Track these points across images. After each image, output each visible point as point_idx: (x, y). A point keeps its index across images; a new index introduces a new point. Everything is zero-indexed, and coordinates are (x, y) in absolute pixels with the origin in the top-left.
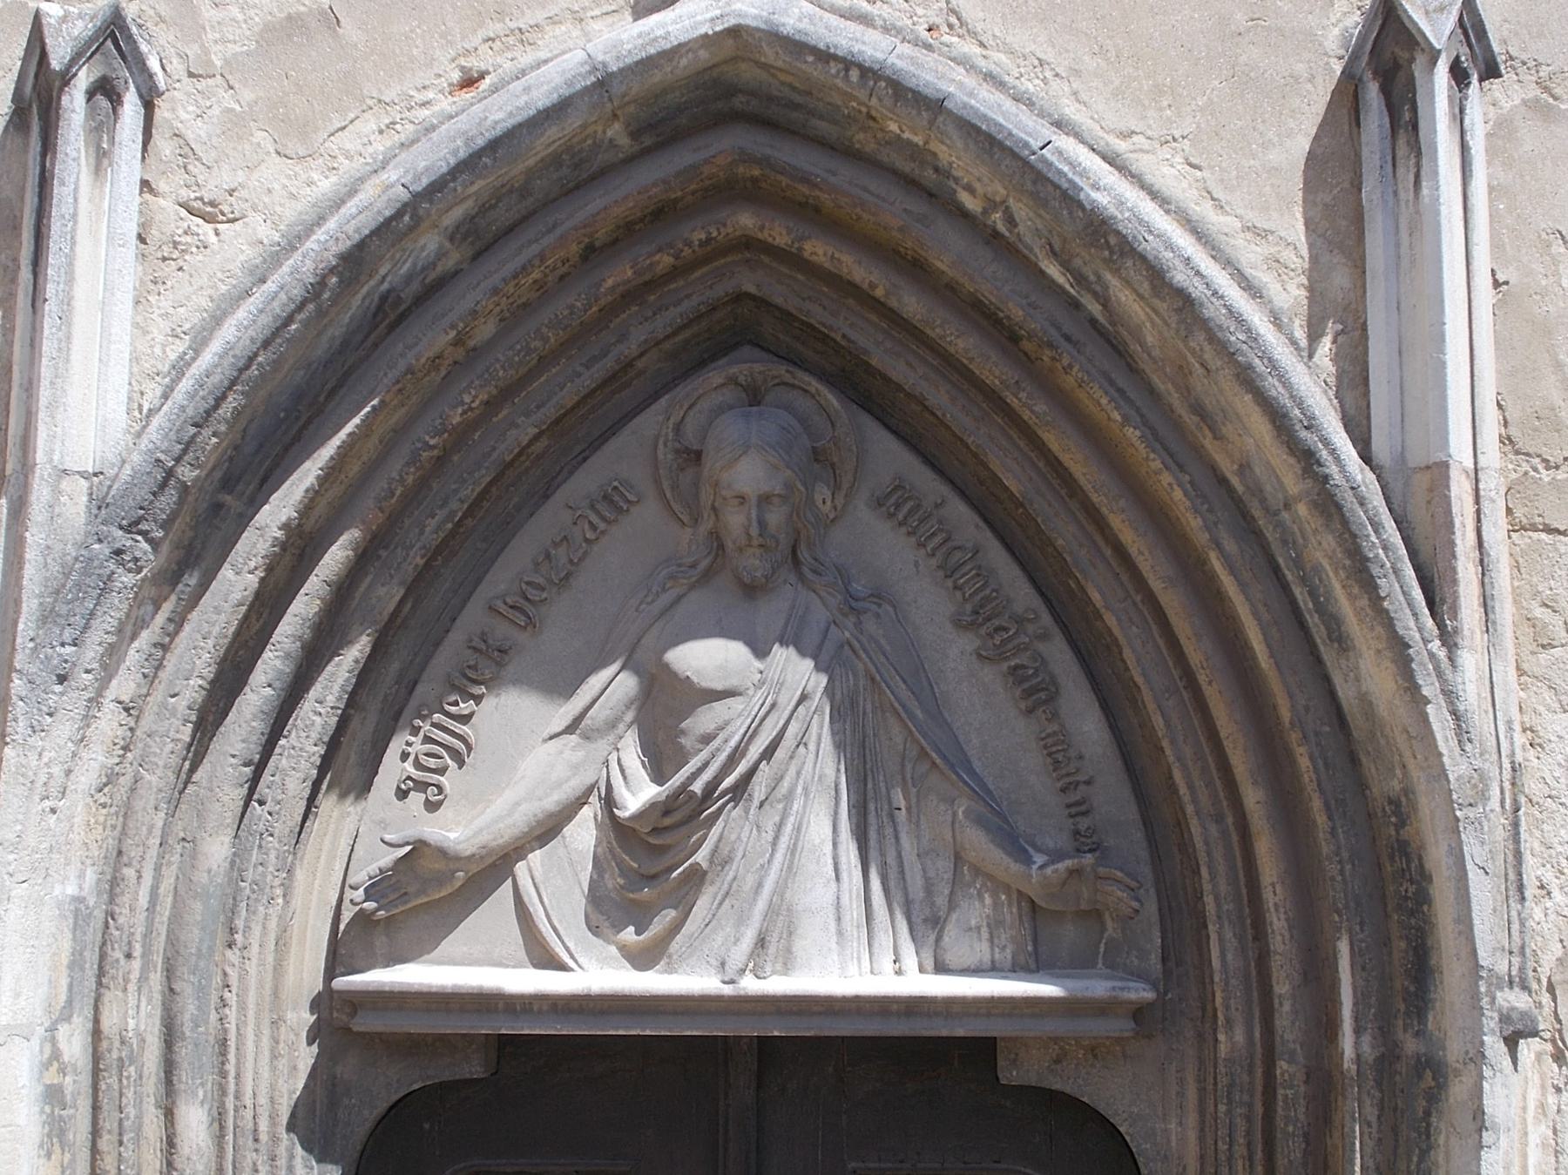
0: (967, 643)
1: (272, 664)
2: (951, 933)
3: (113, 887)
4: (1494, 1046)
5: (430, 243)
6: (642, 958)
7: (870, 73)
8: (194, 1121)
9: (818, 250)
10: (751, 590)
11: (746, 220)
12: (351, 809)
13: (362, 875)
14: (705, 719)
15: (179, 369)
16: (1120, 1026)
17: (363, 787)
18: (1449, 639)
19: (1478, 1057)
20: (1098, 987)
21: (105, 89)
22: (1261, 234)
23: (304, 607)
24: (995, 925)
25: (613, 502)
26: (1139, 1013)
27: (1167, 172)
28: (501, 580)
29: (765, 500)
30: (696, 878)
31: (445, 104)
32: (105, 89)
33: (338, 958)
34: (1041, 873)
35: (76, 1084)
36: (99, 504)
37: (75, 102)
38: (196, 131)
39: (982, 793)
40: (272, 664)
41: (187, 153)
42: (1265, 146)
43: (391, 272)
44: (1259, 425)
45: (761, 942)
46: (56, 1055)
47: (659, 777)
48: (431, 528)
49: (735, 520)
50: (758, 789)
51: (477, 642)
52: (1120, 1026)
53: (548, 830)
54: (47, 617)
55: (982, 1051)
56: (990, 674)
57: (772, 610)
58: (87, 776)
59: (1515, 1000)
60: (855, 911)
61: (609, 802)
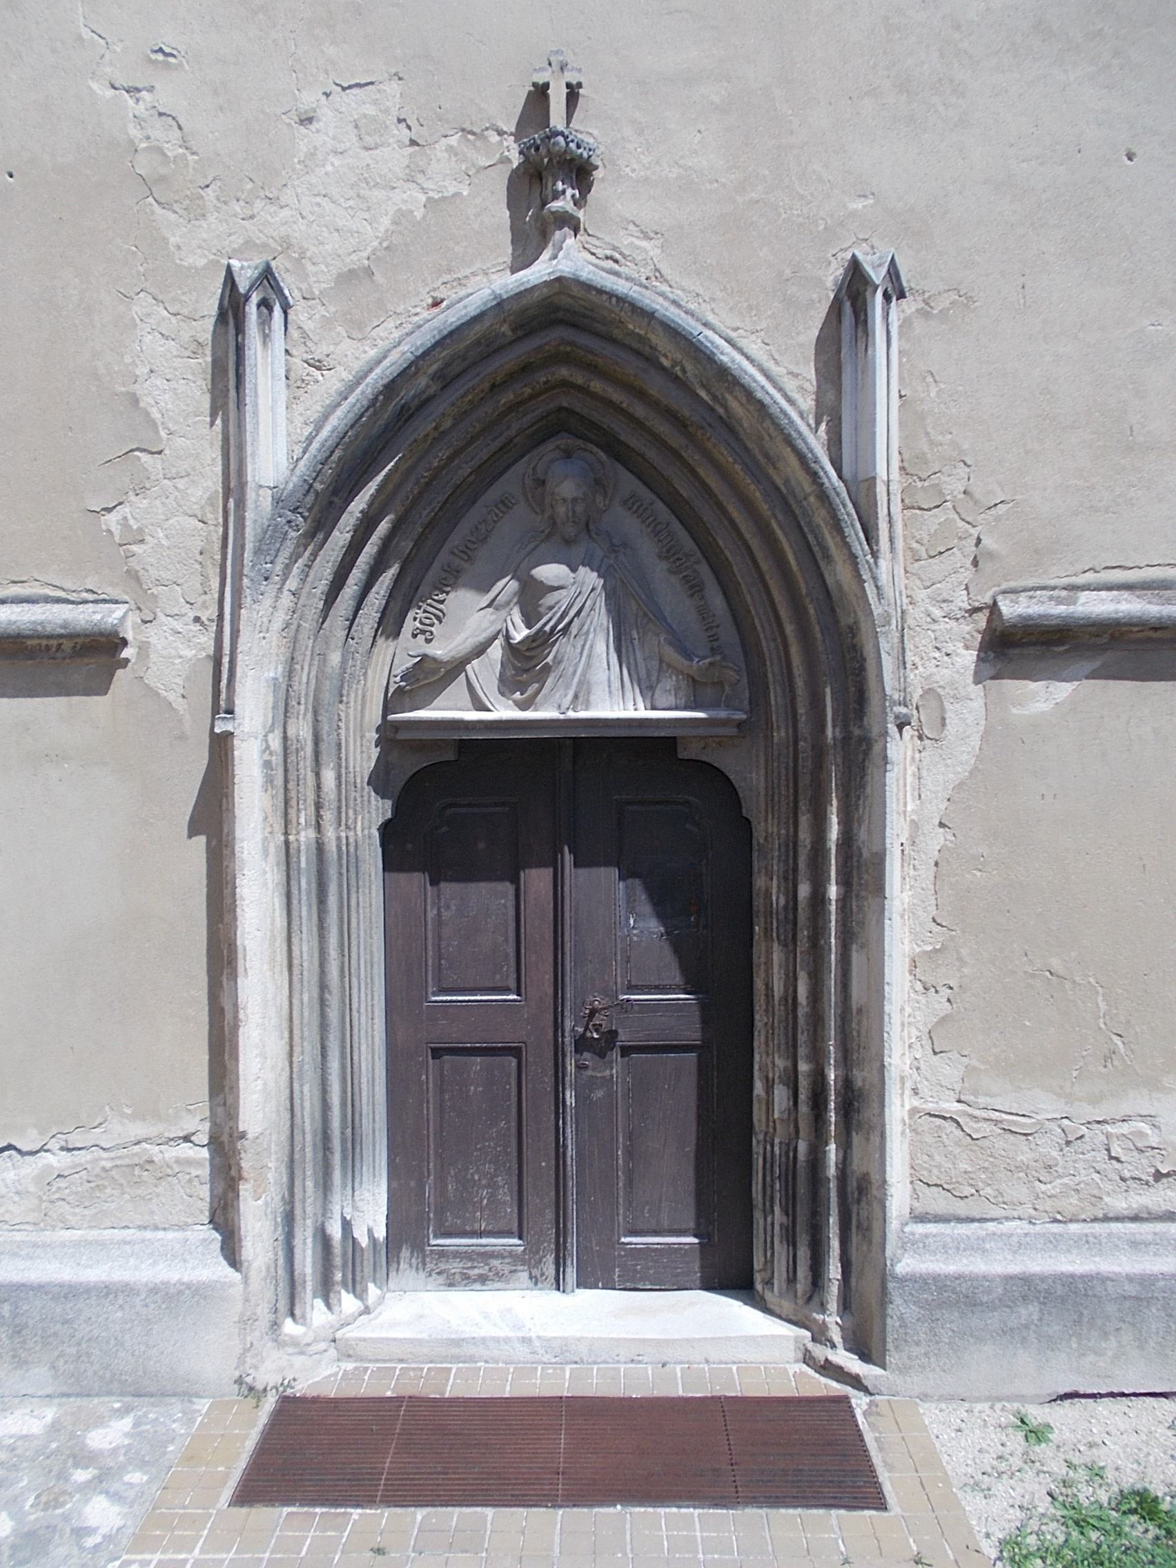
0: (664, 565)
1: (357, 575)
2: (658, 692)
3: (290, 674)
4: (892, 728)
5: (423, 381)
6: (523, 706)
7: (621, 300)
8: (329, 776)
9: (597, 386)
10: (568, 542)
11: (564, 372)
12: (392, 644)
13: (398, 670)
14: (550, 599)
15: (310, 440)
16: (731, 731)
17: (396, 634)
18: (875, 555)
19: (885, 733)
20: (722, 714)
21: (265, 304)
22: (796, 376)
23: (370, 549)
24: (677, 689)
25: (505, 504)
26: (740, 725)
28: (455, 540)
29: (575, 500)
30: (547, 669)
31: (426, 314)
33: (387, 709)
34: (696, 666)
35: (277, 760)
36: (277, 501)
37: (252, 309)
38: (309, 326)
39: (670, 630)
40: (357, 575)
41: (305, 336)
42: (798, 334)
43: (406, 394)
44: (793, 461)
45: (576, 697)
46: (268, 747)
47: (529, 627)
48: (425, 515)
49: (561, 510)
50: (574, 629)
51: (446, 568)
52: (731, 731)
53: (480, 650)
54: (257, 551)
55: (670, 744)
56: (674, 580)
57: (579, 551)
58: (277, 624)
59: (903, 710)
60: (616, 683)
61: (508, 637)
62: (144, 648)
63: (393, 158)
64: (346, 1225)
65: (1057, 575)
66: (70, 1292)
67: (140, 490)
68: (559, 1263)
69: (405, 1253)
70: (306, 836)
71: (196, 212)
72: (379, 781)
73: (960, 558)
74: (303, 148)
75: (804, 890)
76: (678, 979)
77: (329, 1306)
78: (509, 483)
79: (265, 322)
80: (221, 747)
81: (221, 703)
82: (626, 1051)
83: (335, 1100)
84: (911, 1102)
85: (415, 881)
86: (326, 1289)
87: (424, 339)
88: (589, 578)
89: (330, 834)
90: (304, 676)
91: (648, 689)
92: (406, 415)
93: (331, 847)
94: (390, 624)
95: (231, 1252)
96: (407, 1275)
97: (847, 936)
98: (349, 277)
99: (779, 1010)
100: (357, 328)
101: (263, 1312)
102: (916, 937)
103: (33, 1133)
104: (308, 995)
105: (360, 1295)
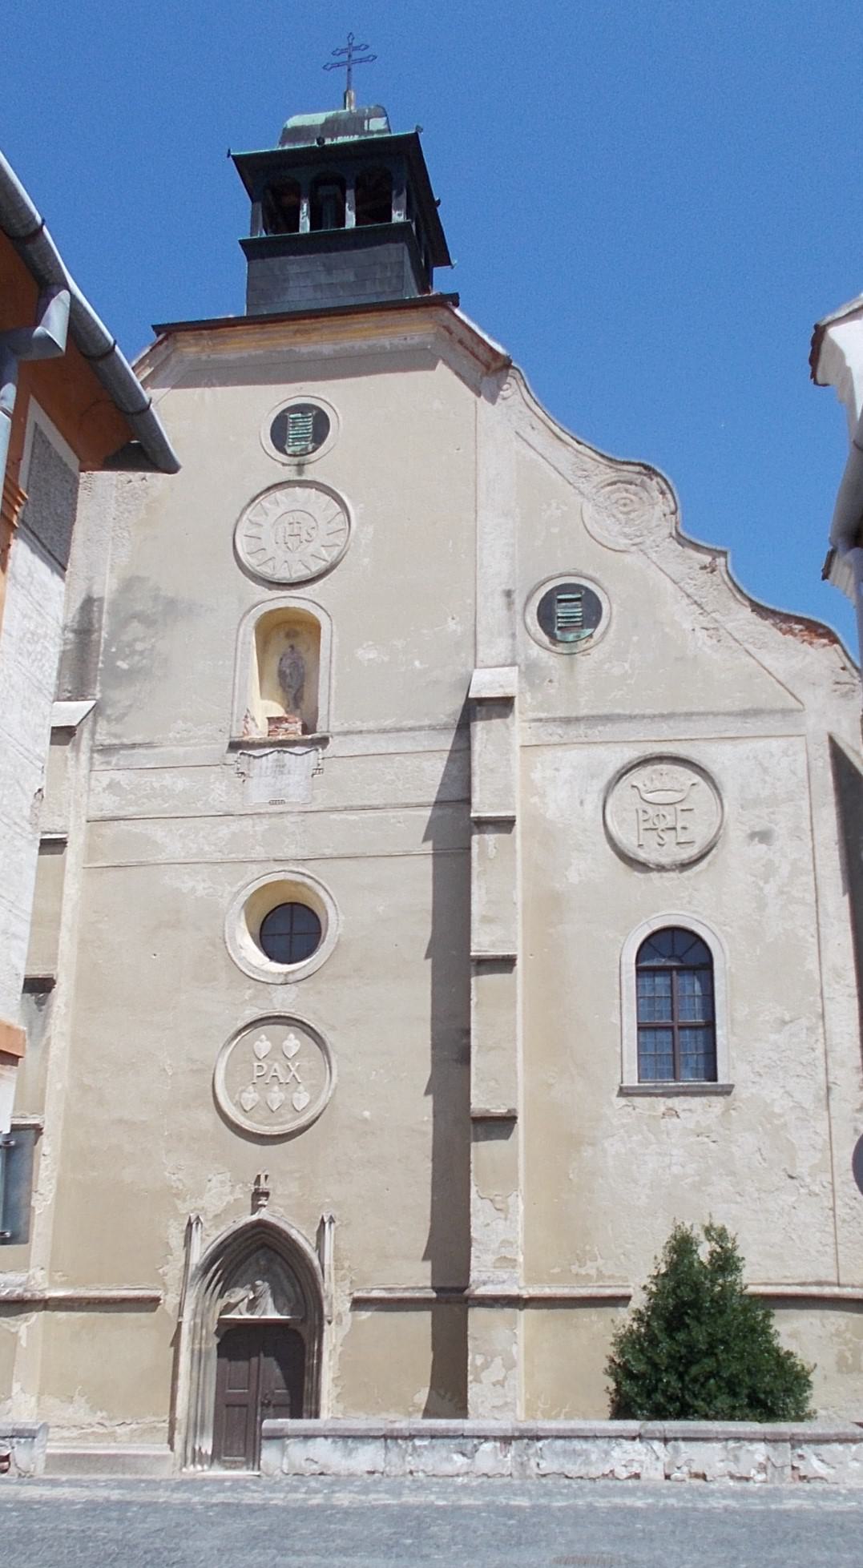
1: (214, 1283)
3: (197, 1307)
6: (252, 1314)
8: (204, 1332)
10: (264, 1274)
17: (222, 1297)
21: (197, 1224)
25: (250, 1265)
28: (238, 1273)
32: (197, 1224)
33: (220, 1315)
37: (194, 1226)
40: (214, 1283)
43: (226, 1243)
53: (243, 1300)
62: (165, 1301)
63: (228, 1189)
64: (200, 1449)
66: (136, 1456)
67: (167, 1264)
68: (254, 1464)
69: (216, 1461)
70: (197, 1347)
71: (184, 1201)
72: (217, 1333)
73: (347, 1282)
74: (208, 1186)
76: (284, 1386)
78: (252, 1259)
79: (197, 1227)
80: (180, 1324)
81: (181, 1315)
82: (274, 1406)
83: (199, 1414)
84: (330, 1415)
85: (225, 1360)
86: (193, 1462)
87: (230, 1232)
88: (267, 1284)
89: (203, 1346)
90: (199, 1308)
91: (280, 1311)
92: (226, 1247)
93: (203, 1350)
94: (221, 1295)
95: (172, 1449)
96: (216, 1465)
98: (216, 1216)
100: (217, 1227)
101: (178, 1466)
102: (334, 1373)
104: (194, 1386)
105: (202, 1465)
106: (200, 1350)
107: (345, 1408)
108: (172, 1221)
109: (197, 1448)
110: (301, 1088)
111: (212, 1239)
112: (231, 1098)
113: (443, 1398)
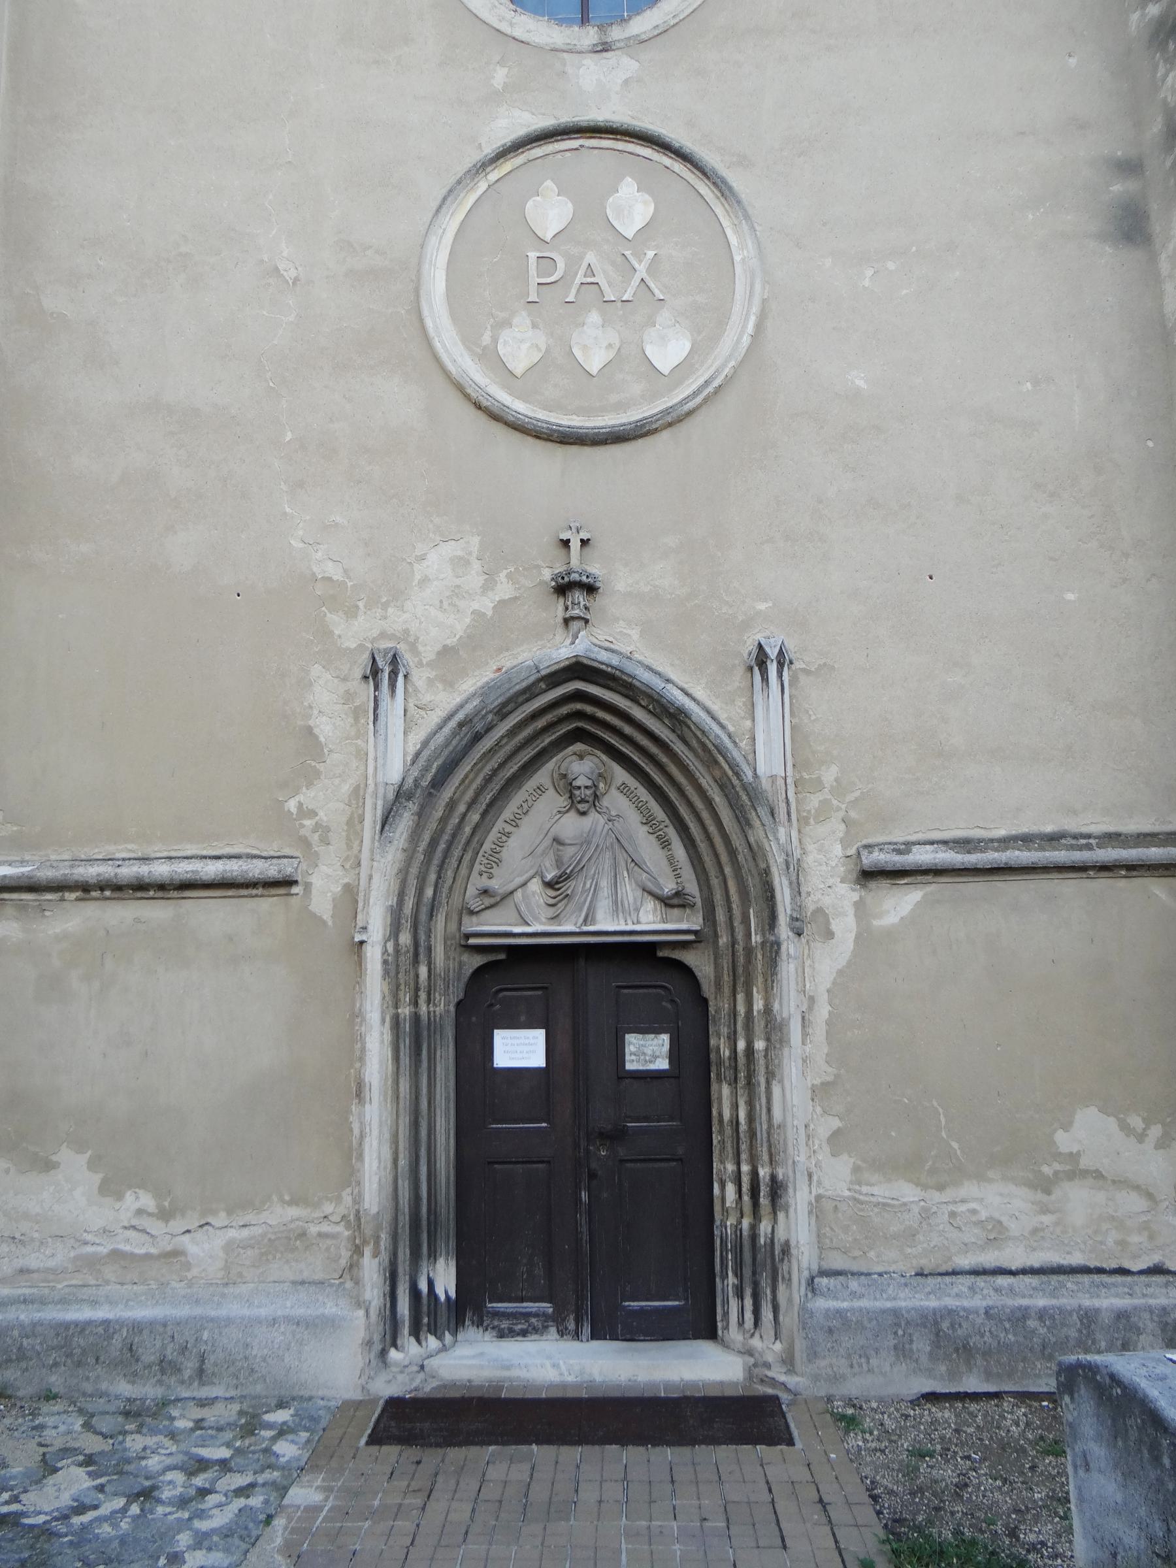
0: (646, 828)
8: (423, 970)
11: (579, 706)
24: (655, 910)
25: (540, 789)
27: (699, 693)
28: (507, 814)
42: (726, 685)
46: (386, 951)
48: (487, 797)
51: (502, 831)
56: (652, 838)
65: (899, 836)
68: (578, 1321)
69: (469, 1314)
70: (405, 1011)
75: (741, 1045)
77: (419, 1341)
86: (416, 1333)
89: (423, 1009)
97: (770, 1075)
98: (446, 652)
99: (728, 1131)
100: (450, 685)
103: (223, 1214)
104: (405, 1121)
105: (440, 1338)
106: (416, 1018)
107: (856, 1169)
108: (316, 670)
109: (423, 1286)
110: (664, 316)
111: (435, 718)
112: (469, 341)
113: (1141, 1137)
